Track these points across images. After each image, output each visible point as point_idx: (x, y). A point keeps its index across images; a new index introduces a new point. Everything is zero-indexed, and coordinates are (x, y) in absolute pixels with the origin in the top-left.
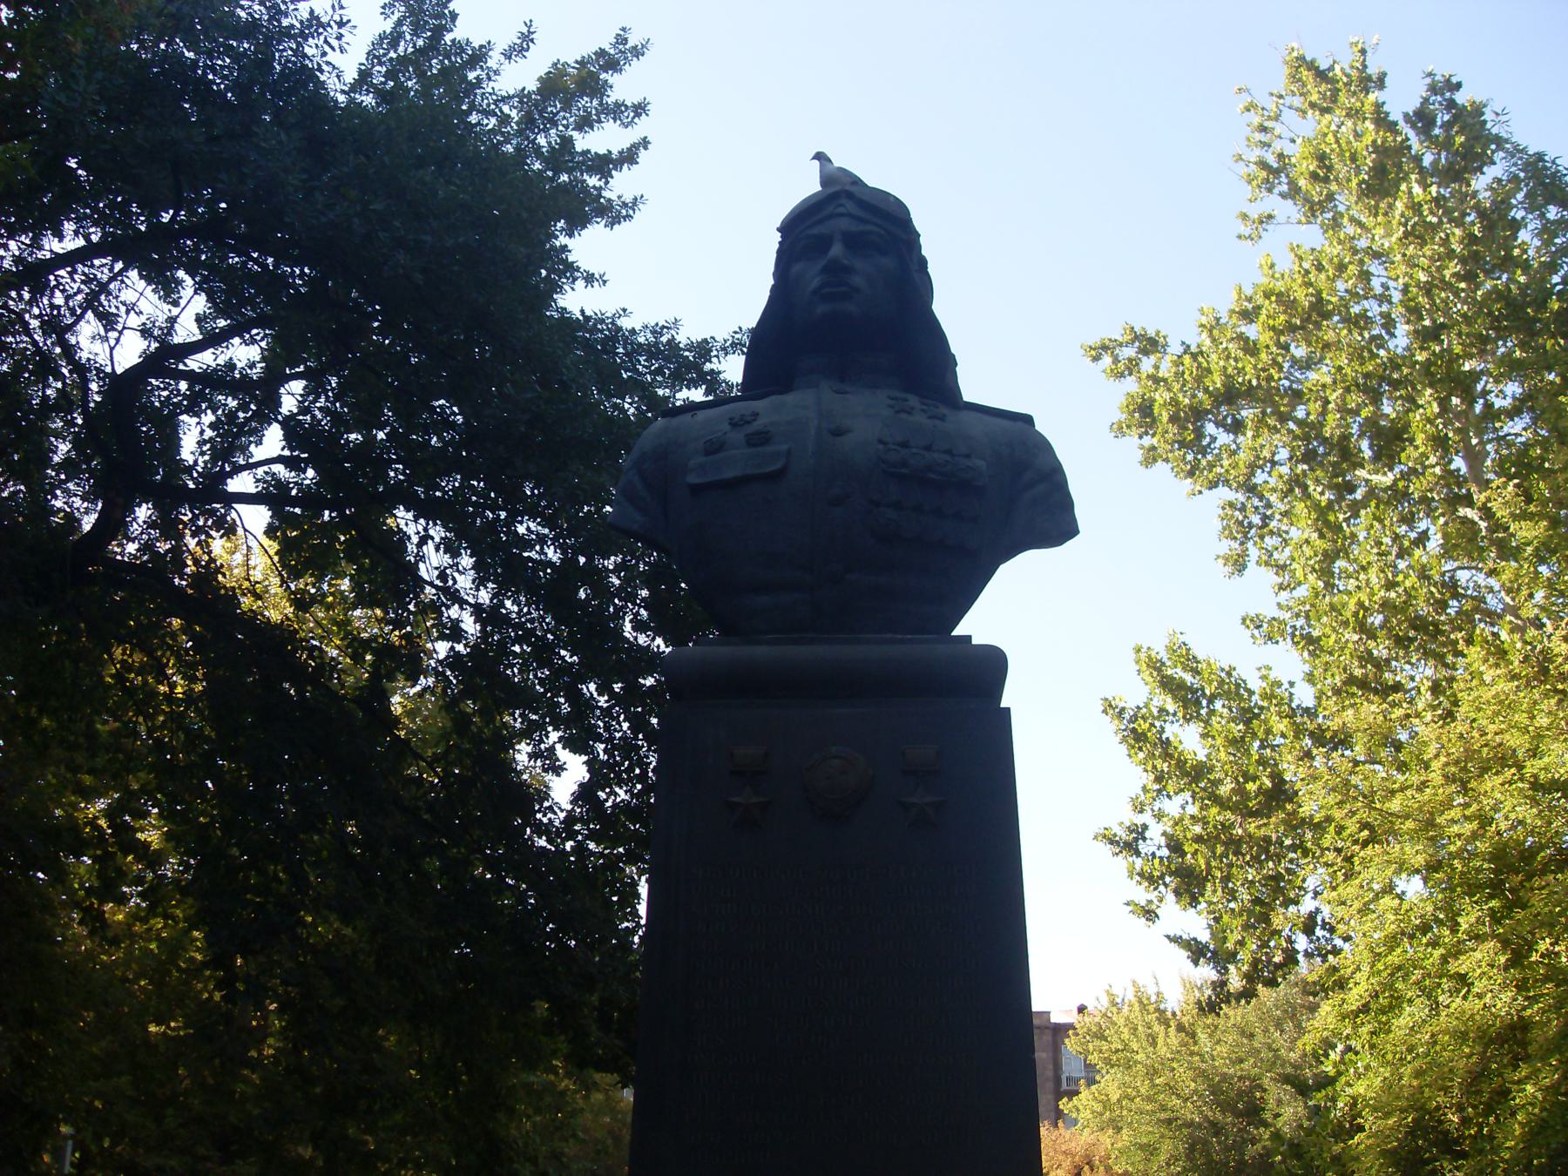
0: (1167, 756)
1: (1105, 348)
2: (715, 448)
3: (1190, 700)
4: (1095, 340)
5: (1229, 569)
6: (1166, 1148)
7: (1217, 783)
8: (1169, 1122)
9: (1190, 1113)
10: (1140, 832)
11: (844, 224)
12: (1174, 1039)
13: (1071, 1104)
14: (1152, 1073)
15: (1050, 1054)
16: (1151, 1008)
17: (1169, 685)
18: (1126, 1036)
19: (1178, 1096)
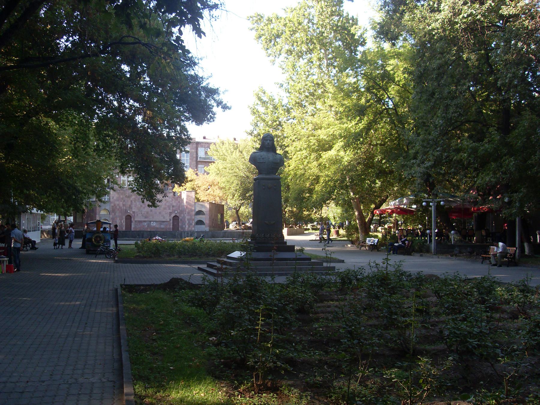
0: (259, 117)
1: (251, 17)
2: (259, 159)
3: (264, 103)
4: (249, 16)
5: (271, 64)
6: (236, 182)
7: (267, 122)
8: (236, 176)
9: (242, 174)
10: (252, 132)
11: (269, 138)
12: (238, 154)
13: (207, 168)
14: (232, 163)
15: (195, 150)
16: (231, 145)
17: (260, 99)
18: (224, 151)
19: (238, 169)
